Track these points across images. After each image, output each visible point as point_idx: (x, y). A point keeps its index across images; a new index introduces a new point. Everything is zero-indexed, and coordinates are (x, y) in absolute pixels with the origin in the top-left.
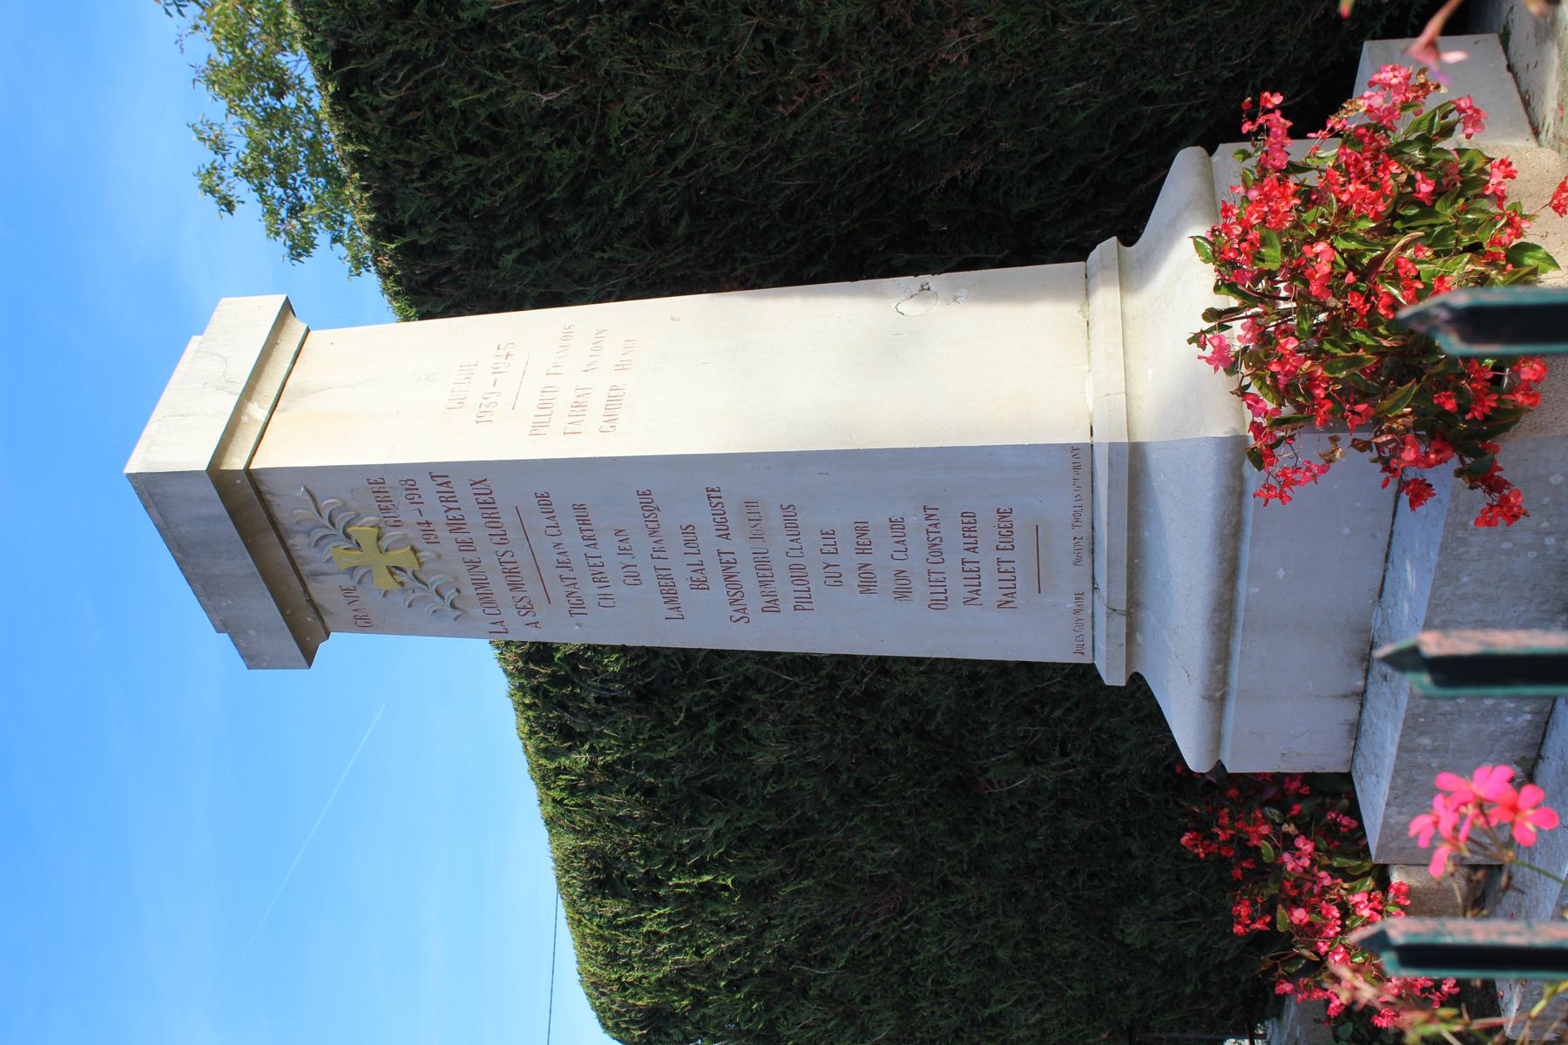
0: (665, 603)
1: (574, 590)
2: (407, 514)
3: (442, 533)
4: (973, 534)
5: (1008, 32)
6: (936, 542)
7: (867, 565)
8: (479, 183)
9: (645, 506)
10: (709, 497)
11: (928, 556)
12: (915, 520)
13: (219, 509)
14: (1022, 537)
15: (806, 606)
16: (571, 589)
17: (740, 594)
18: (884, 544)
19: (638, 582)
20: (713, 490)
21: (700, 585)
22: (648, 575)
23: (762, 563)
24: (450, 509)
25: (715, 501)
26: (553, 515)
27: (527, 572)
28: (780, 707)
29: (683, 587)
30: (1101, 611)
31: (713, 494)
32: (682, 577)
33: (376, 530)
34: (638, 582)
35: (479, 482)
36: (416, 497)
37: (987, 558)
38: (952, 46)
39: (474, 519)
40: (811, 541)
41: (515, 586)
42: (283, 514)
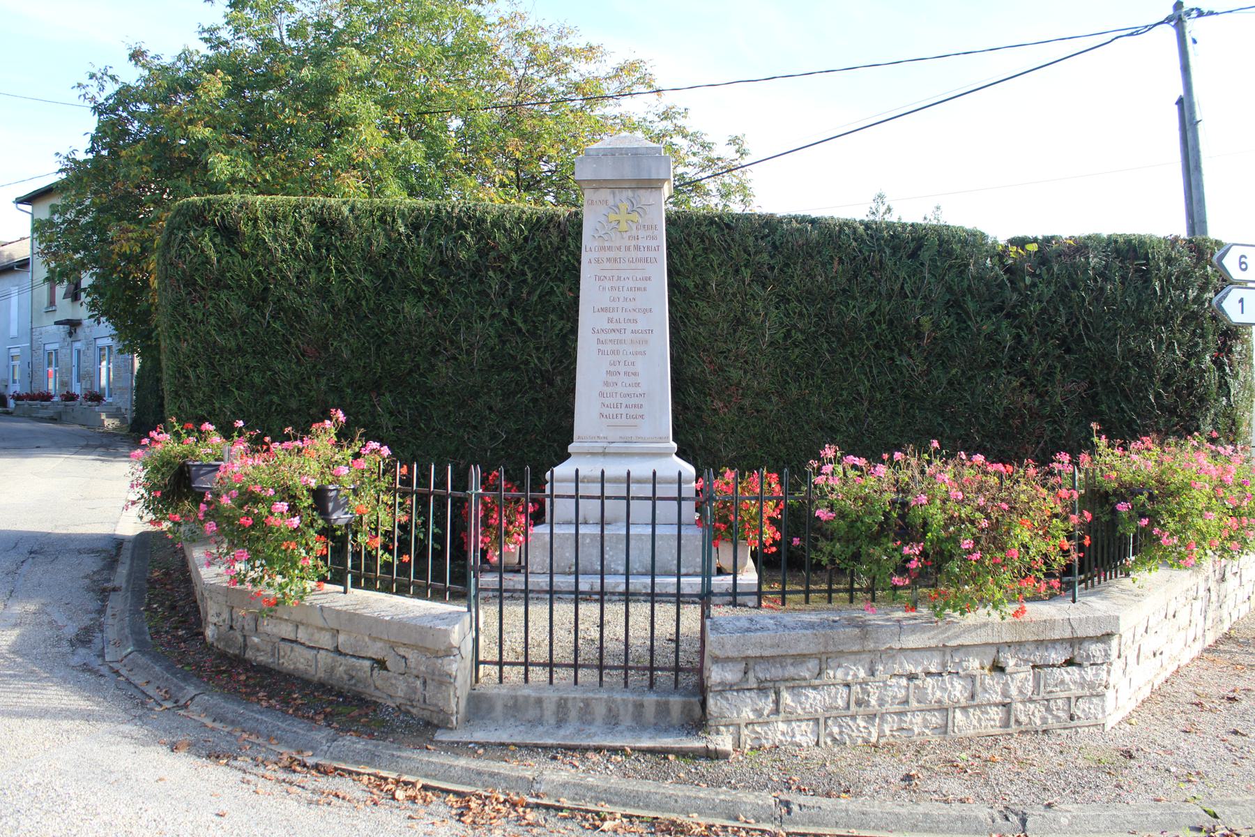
2: (642, 233)
3: (633, 243)
5: (723, 420)
8: (682, 256)
12: (639, 390)
13: (654, 176)
14: (631, 421)
18: (632, 379)
21: (610, 320)
22: (614, 305)
23: (620, 342)
27: (616, 266)
28: (435, 317)
29: (609, 315)
30: (605, 445)
32: (615, 316)
37: (623, 411)
38: (718, 404)
39: (640, 254)
40: (631, 358)
41: (609, 260)
42: (642, 192)
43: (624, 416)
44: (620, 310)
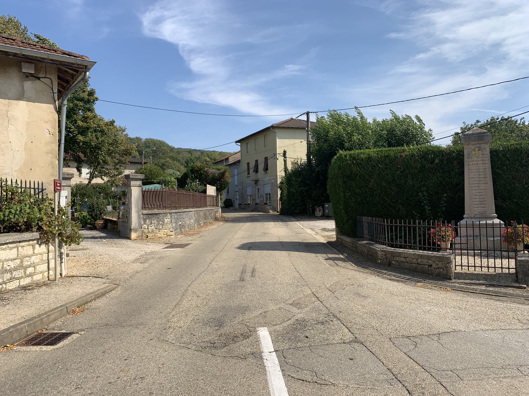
43: (480, 207)
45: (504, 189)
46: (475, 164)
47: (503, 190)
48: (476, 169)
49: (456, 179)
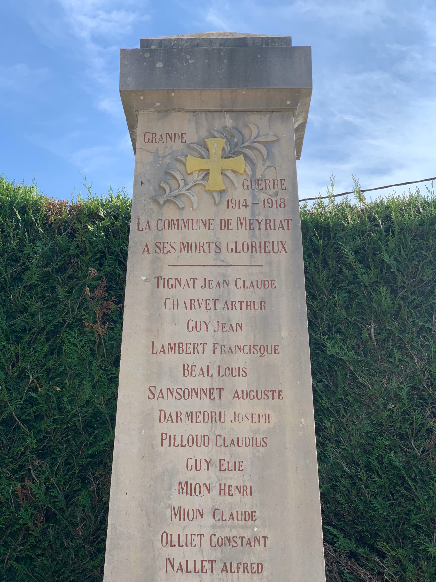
0: (169, 344)
1: (182, 285)
4: (241, 570)
6: (233, 543)
7: (209, 490)
9: (266, 349)
10: (273, 391)
11: (217, 536)
15: (166, 442)
16: (183, 282)
17: (179, 397)
19: (190, 329)
20: (280, 395)
24: (260, 224)
25: (270, 394)
26: (255, 286)
29: (190, 359)
31: (276, 395)
33: (242, 172)
34: (190, 329)
35: (284, 248)
36: (270, 205)
44: (209, 348)
45: (369, 469)
46: (199, 247)
47: (363, 475)
48: (207, 283)
49: (87, 386)
